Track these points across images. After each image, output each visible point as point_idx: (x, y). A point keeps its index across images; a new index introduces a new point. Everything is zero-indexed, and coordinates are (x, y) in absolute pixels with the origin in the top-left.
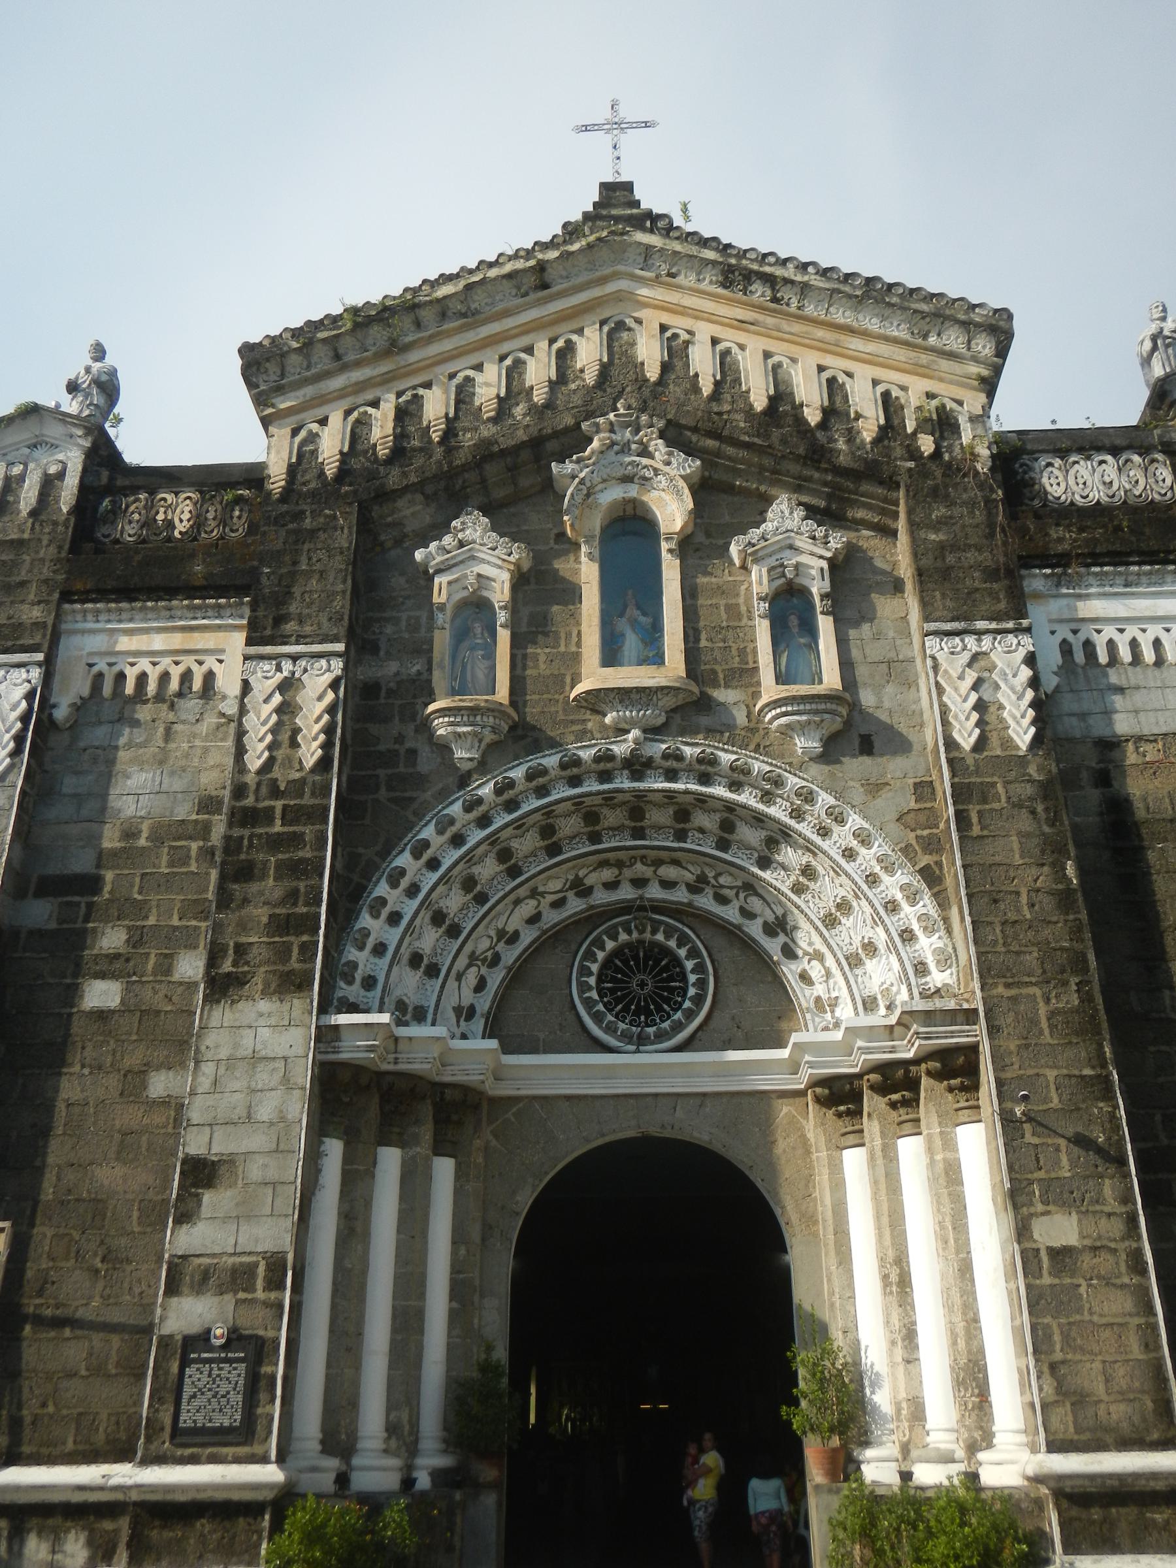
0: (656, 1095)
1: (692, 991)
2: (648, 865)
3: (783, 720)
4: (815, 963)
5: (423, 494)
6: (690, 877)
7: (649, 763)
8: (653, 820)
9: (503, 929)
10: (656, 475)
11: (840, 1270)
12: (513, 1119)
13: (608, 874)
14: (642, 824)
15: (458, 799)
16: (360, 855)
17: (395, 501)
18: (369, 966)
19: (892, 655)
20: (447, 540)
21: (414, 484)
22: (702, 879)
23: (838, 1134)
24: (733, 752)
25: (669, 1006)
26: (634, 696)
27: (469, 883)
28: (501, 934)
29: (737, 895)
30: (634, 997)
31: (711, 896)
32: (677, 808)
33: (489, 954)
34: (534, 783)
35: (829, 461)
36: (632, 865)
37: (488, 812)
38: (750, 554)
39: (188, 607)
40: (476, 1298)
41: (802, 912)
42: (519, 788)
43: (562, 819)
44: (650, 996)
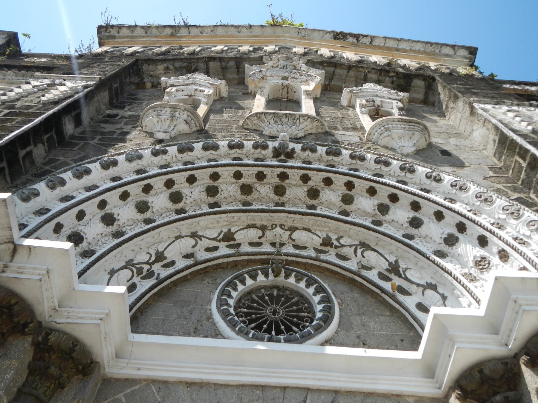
0: (285, 388)
1: (319, 315)
2: (286, 230)
4: (429, 292)
6: (317, 241)
7: (290, 155)
8: (291, 196)
9: (163, 253)
10: (301, 76)
12: (124, 400)
13: (254, 234)
15: (149, 148)
16: (59, 160)
17: (156, 65)
18: (26, 218)
19: (449, 132)
21: (170, 60)
22: (327, 242)
24: (351, 149)
25: (298, 327)
26: (284, 120)
27: (142, 207)
28: (160, 257)
29: (355, 252)
30: (267, 320)
31: (334, 256)
32: (310, 187)
33: (146, 267)
34: (208, 153)
35: (394, 72)
36: (273, 229)
37: (169, 163)
39: (16, 76)
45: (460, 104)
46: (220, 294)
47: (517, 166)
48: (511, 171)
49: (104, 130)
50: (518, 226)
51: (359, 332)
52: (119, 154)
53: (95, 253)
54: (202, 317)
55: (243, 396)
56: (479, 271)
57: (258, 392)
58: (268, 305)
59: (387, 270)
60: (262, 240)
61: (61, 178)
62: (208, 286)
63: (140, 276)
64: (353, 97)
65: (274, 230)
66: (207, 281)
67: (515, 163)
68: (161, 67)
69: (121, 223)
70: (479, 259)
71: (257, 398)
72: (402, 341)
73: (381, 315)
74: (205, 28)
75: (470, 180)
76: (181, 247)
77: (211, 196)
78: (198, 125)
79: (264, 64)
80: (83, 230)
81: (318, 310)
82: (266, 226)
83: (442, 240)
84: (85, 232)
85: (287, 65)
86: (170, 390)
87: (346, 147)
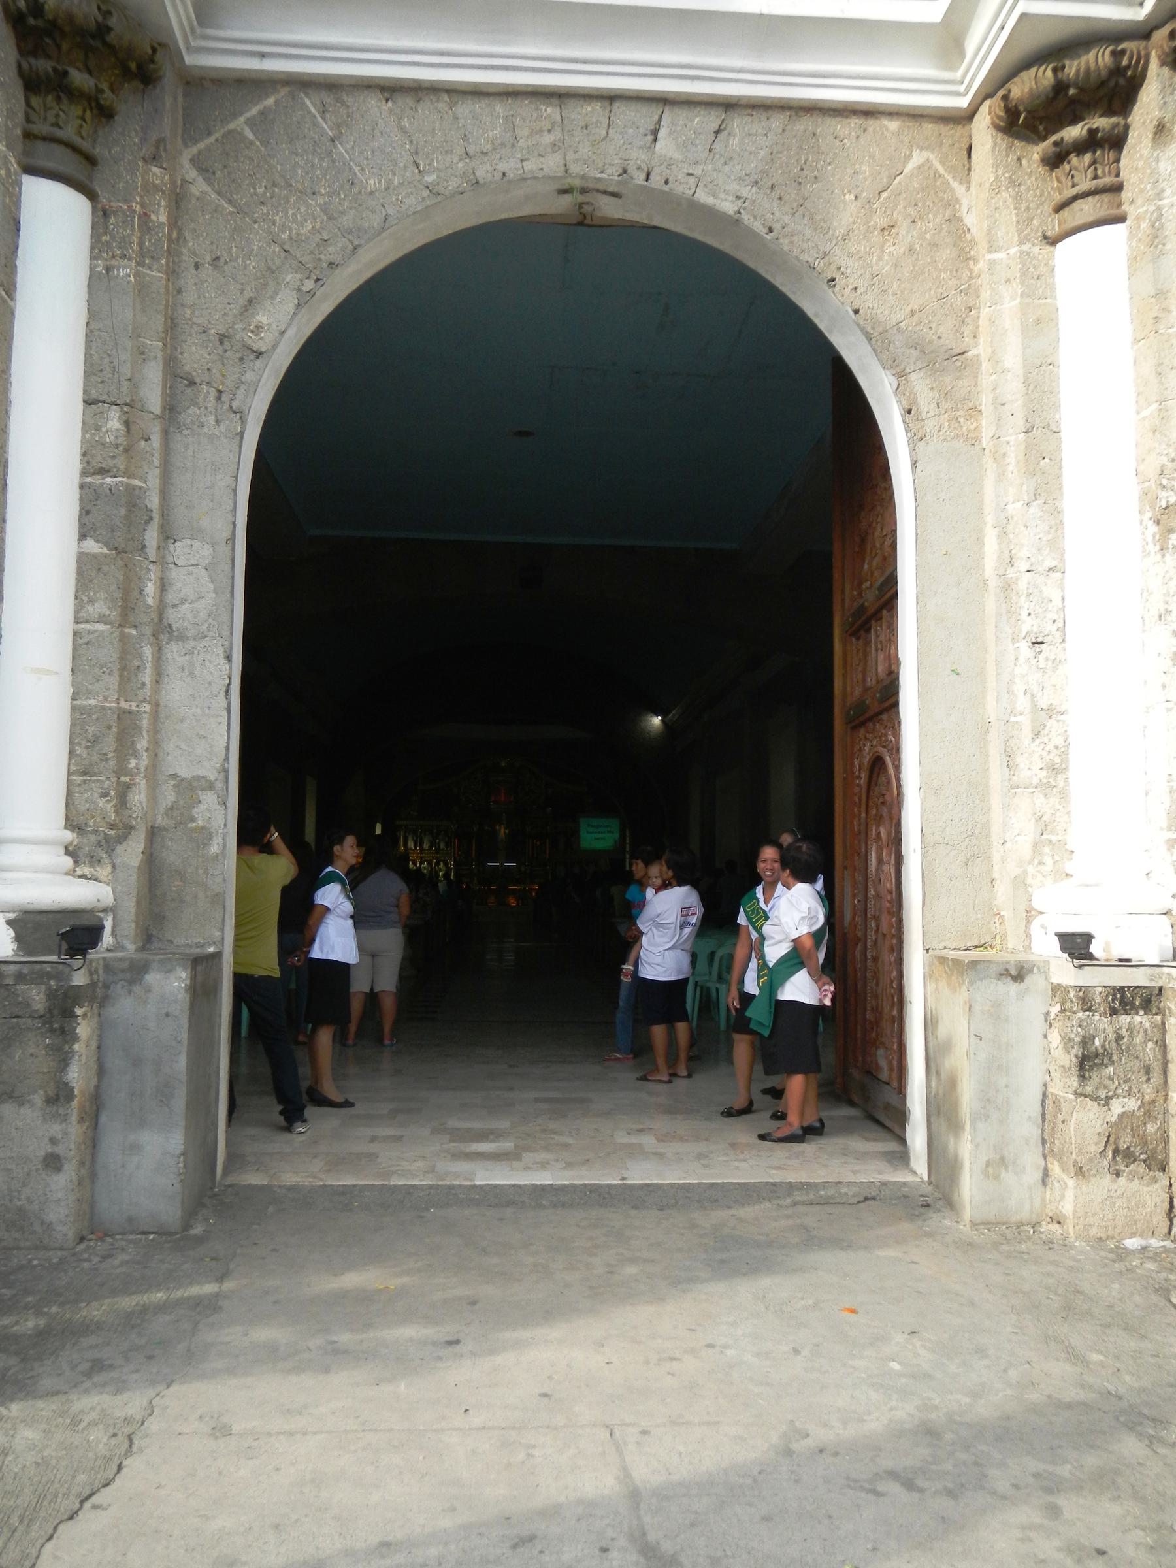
11: (1034, 509)
12: (251, 136)
23: (1048, 208)
40: (152, 536)
55: (518, 121)
57: (549, 110)
71: (549, 126)
86: (348, 107)
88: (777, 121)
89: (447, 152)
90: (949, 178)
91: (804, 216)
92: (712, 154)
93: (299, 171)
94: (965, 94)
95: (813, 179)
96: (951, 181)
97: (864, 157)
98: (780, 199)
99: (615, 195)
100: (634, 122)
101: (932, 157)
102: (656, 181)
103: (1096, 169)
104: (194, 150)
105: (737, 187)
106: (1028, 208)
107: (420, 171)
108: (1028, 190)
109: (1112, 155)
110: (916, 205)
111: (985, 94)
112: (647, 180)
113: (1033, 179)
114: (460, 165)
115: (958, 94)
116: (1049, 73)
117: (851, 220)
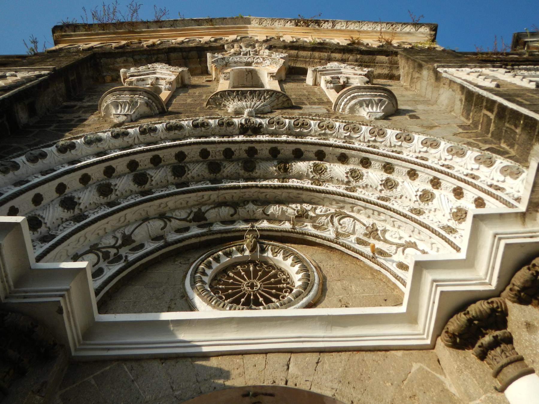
3: (353, 102)
4: (409, 250)
5: (133, 58)
10: (264, 61)
12: (93, 382)
13: (225, 211)
14: (254, 174)
17: (116, 58)
20: (141, 68)
28: (127, 240)
29: (332, 221)
30: (245, 294)
33: (113, 251)
36: (245, 205)
38: (319, 71)
41: (389, 209)
42: (161, 134)
43: (191, 165)
44: (260, 294)
45: (425, 73)
46: (193, 272)
47: (485, 119)
48: (480, 126)
49: (61, 119)
50: (491, 173)
51: (341, 297)
52: (77, 138)
53: (55, 237)
54: (175, 296)
56: (457, 222)
57: (238, 361)
58: (245, 280)
59: (366, 235)
60: (235, 217)
61: (14, 162)
62: (181, 266)
63: (107, 261)
64: (318, 75)
65: (246, 207)
66: (179, 262)
67: (483, 117)
68: (120, 60)
69: (82, 207)
70: (455, 210)
71: (237, 366)
72: (386, 300)
73: (362, 279)
74: (164, 23)
75: (441, 137)
76: (150, 229)
77: (178, 176)
78: (160, 107)
79: (226, 51)
80: (41, 214)
81: (297, 279)
82: (238, 203)
83: (418, 197)
84: (44, 216)
85: (249, 51)
86: (143, 367)
87: (314, 118)
88: (344, 356)
89: (187, 381)
90: (434, 373)
91: (368, 394)
92: (316, 372)
93: (113, 396)
94: (427, 338)
95: (368, 378)
96: (436, 374)
97: (390, 368)
98: (354, 388)
99: (271, 395)
100: (278, 362)
101: (422, 365)
102: (290, 385)
103: (505, 353)
104: (64, 391)
105: (331, 384)
106: (480, 377)
107: (173, 390)
108: (476, 369)
109: (509, 346)
110: (423, 385)
111: (437, 335)
112: (286, 383)
113: (476, 365)
114: (193, 386)
115: (423, 339)
116: (463, 316)
117: (393, 394)
